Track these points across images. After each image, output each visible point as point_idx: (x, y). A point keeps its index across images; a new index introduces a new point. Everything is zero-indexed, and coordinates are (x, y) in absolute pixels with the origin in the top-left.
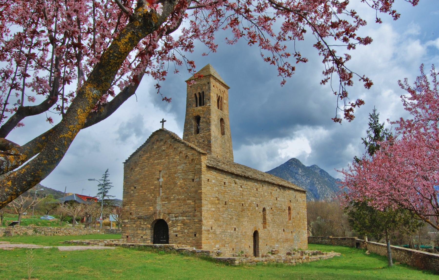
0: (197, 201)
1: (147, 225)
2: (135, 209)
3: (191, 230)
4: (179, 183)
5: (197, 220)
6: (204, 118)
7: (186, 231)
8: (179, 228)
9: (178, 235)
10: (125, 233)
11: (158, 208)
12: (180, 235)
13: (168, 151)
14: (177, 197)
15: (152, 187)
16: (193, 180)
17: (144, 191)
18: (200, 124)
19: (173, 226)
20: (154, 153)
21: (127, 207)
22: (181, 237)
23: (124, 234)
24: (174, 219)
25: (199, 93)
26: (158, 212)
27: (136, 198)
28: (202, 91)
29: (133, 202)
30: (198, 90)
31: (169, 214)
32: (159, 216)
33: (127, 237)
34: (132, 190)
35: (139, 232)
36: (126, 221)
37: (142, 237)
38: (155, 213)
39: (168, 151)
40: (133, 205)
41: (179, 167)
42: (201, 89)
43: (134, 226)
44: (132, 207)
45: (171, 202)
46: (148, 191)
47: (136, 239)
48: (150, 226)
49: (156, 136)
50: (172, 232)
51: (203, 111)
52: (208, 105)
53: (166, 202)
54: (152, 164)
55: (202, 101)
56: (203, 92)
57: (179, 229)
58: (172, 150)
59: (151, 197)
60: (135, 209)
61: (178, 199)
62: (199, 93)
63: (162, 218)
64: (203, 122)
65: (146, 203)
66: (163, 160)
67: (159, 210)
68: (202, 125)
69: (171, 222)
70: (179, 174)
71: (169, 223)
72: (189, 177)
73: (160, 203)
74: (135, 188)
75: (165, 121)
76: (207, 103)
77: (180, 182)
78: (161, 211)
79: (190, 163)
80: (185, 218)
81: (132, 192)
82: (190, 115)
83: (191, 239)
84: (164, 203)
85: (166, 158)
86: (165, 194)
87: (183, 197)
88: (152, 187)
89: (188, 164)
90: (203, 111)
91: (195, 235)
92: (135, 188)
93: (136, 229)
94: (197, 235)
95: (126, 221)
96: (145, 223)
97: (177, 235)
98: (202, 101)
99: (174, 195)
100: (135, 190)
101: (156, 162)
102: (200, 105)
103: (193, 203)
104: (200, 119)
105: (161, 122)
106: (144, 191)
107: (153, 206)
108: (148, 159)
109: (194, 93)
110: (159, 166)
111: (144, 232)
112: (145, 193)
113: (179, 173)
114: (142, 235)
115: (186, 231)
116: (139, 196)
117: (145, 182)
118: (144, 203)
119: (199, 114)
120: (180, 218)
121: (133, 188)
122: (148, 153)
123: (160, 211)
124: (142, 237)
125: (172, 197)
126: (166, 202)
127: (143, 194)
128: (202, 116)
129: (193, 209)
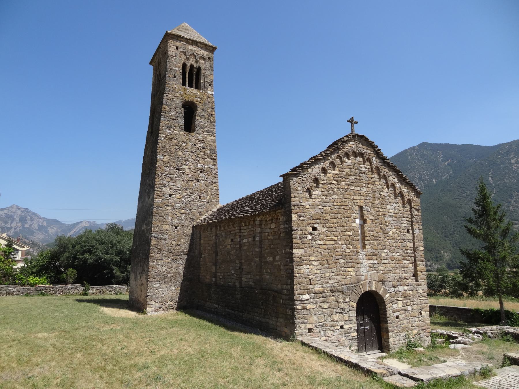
0: (418, 263)
1: (351, 303)
2: (318, 271)
3: (415, 307)
4: (391, 232)
5: (421, 291)
6: (204, 110)
7: (409, 308)
8: (400, 306)
9: (400, 316)
10: (306, 323)
11: (364, 271)
12: (403, 316)
13: (371, 176)
14: (390, 254)
15: (349, 233)
16: (408, 232)
17: (335, 238)
18: (197, 117)
19: (393, 302)
20: (348, 171)
21: (304, 267)
22: (405, 319)
23: (303, 326)
24: (393, 289)
25: (192, 66)
26: (363, 278)
27: (319, 250)
28: (198, 65)
29: (313, 258)
30: (191, 59)
31: (382, 282)
32: (370, 286)
33: (310, 330)
34: (311, 234)
35: (336, 317)
36: (306, 297)
37: (342, 327)
38: (359, 281)
39: (371, 176)
40: (315, 263)
41: (389, 207)
42: (197, 62)
43: (325, 306)
44: (311, 267)
45: (383, 261)
46: (342, 240)
47: (329, 333)
48: (355, 305)
49: (352, 144)
50: (391, 311)
51: (201, 98)
52: (209, 92)
53: (375, 262)
54: (346, 190)
55: (194, 81)
56: (199, 69)
57: (400, 306)
58: (377, 177)
59: (348, 251)
60: (318, 271)
61: (392, 259)
62: (192, 66)
63: (374, 289)
64: (202, 116)
65: (343, 261)
66: (365, 189)
67: (364, 274)
68: (199, 121)
69: (388, 295)
70: (390, 219)
71: (387, 297)
72: (403, 225)
73: (366, 262)
74: (315, 229)
75: (356, 123)
76: (207, 88)
77: (392, 231)
78: (369, 277)
79: (403, 204)
80: (406, 288)
81: (309, 237)
82: (178, 95)
83: (417, 320)
84: (371, 262)
85: (369, 186)
86: (372, 248)
87: (398, 254)
88: (349, 233)
89: (401, 205)
90: (201, 98)
91: (421, 314)
92: (315, 229)
93: (328, 311)
94: (423, 313)
95: (306, 297)
96: (347, 300)
97: (397, 317)
98: (194, 81)
99: (385, 251)
100: (316, 233)
101: (351, 188)
102: (191, 86)
103: (411, 265)
104: (197, 110)
105: (349, 121)
106: (335, 238)
107: (353, 267)
108: (338, 179)
109: (183, 61)
110: (358, 198)
111: (346, 317)
112: (337, 243)
113: (391, 216)
114: (341, 323)
115: (409, 308)
116: (325, 247)
117: (335, 221)
118: (336, 261)
119: (194, 99)
120: (401, 288)
121: (310, 229)
122: (337, 169)
123: (366, 276)
124: (342, 327)
125: (383, 254)
126: (375, 262)
127: (333, 243)
128: (200, 105)
129: (412, 274)
